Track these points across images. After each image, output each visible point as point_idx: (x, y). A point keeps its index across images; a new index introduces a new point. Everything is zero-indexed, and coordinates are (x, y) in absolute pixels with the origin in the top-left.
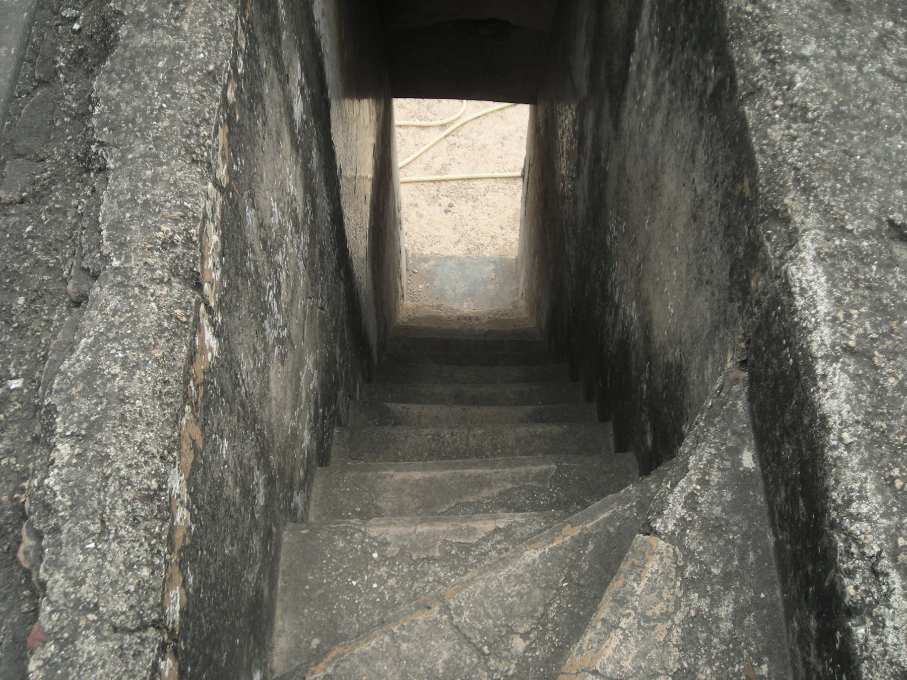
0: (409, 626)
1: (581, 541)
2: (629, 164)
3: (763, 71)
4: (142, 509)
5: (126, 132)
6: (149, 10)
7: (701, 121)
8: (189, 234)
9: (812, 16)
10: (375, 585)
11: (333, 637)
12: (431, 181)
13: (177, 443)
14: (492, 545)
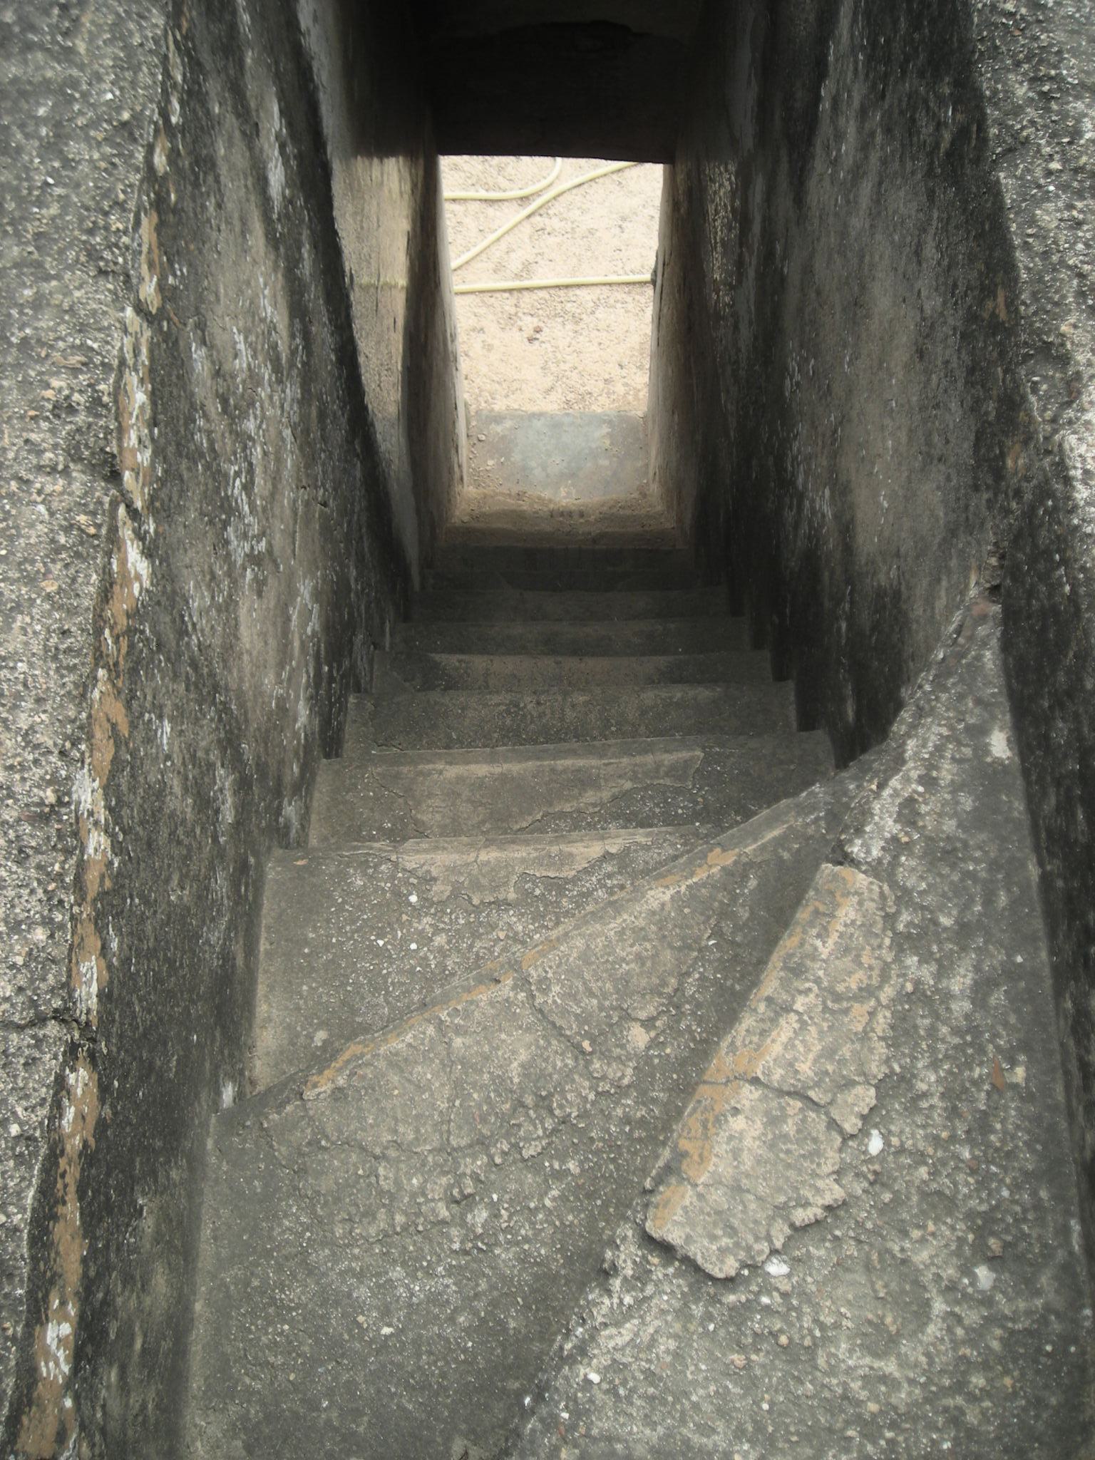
0: (465, 1010)
1: (736, 875)
2: (819, 264)
3: (1031, 112)
4: (32, 836)
7: (931, 195)
8: (97, 391)
10: (413, 946)
11: (349, 1028)
12: (504, 291)
13: (86, 730)
14: (599, 880)
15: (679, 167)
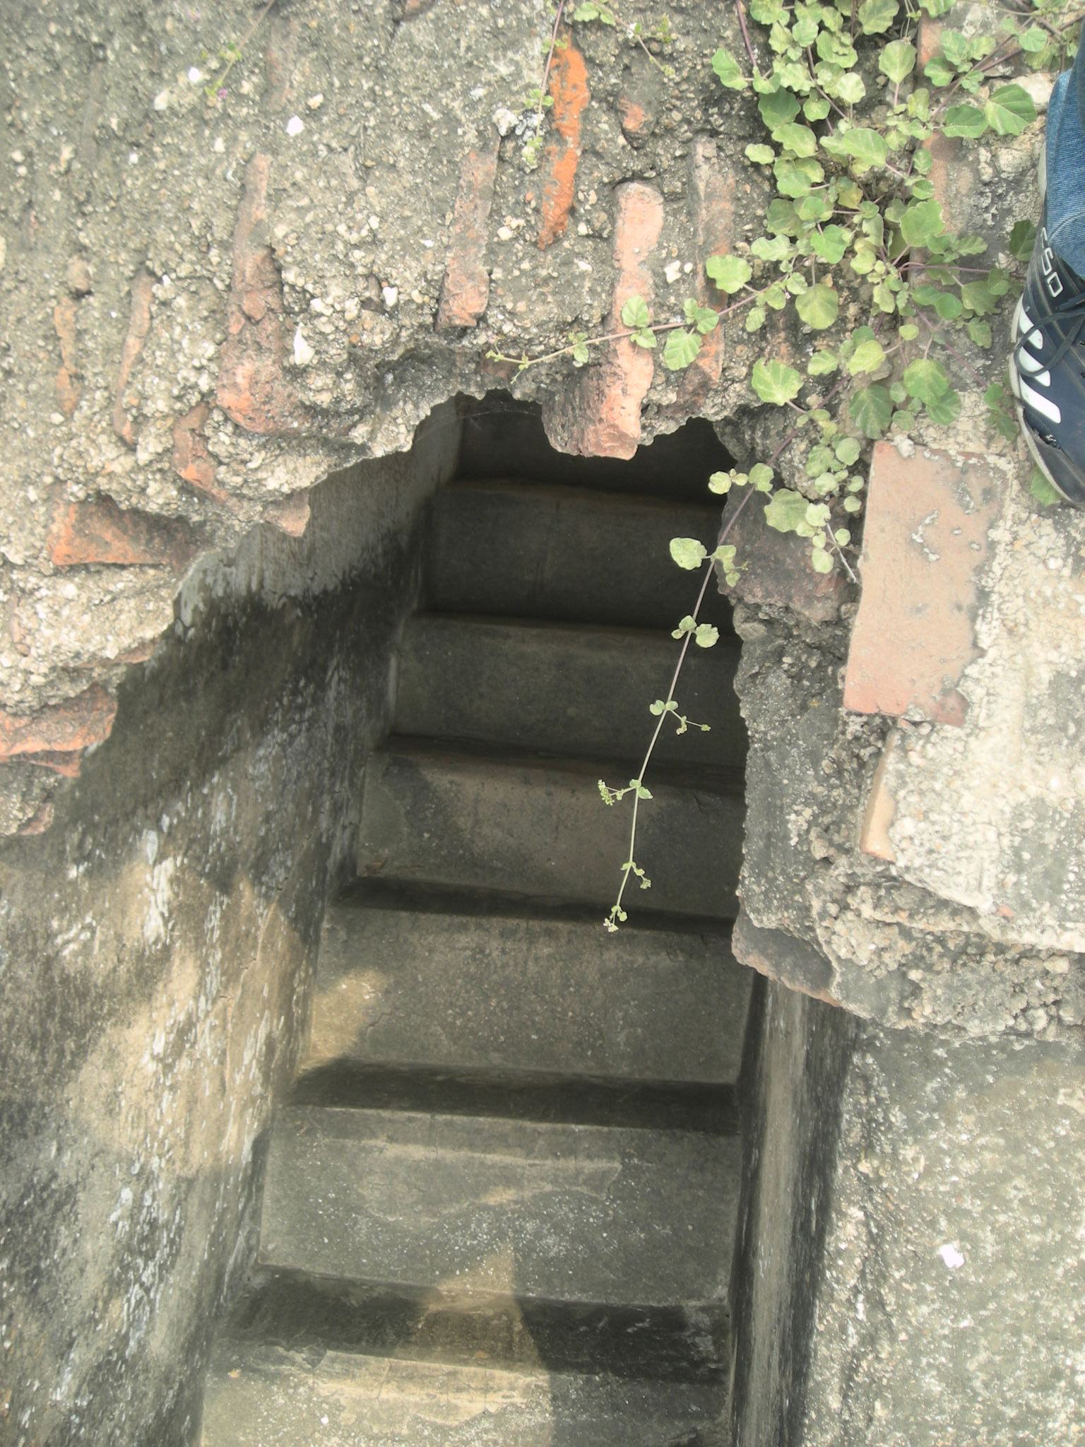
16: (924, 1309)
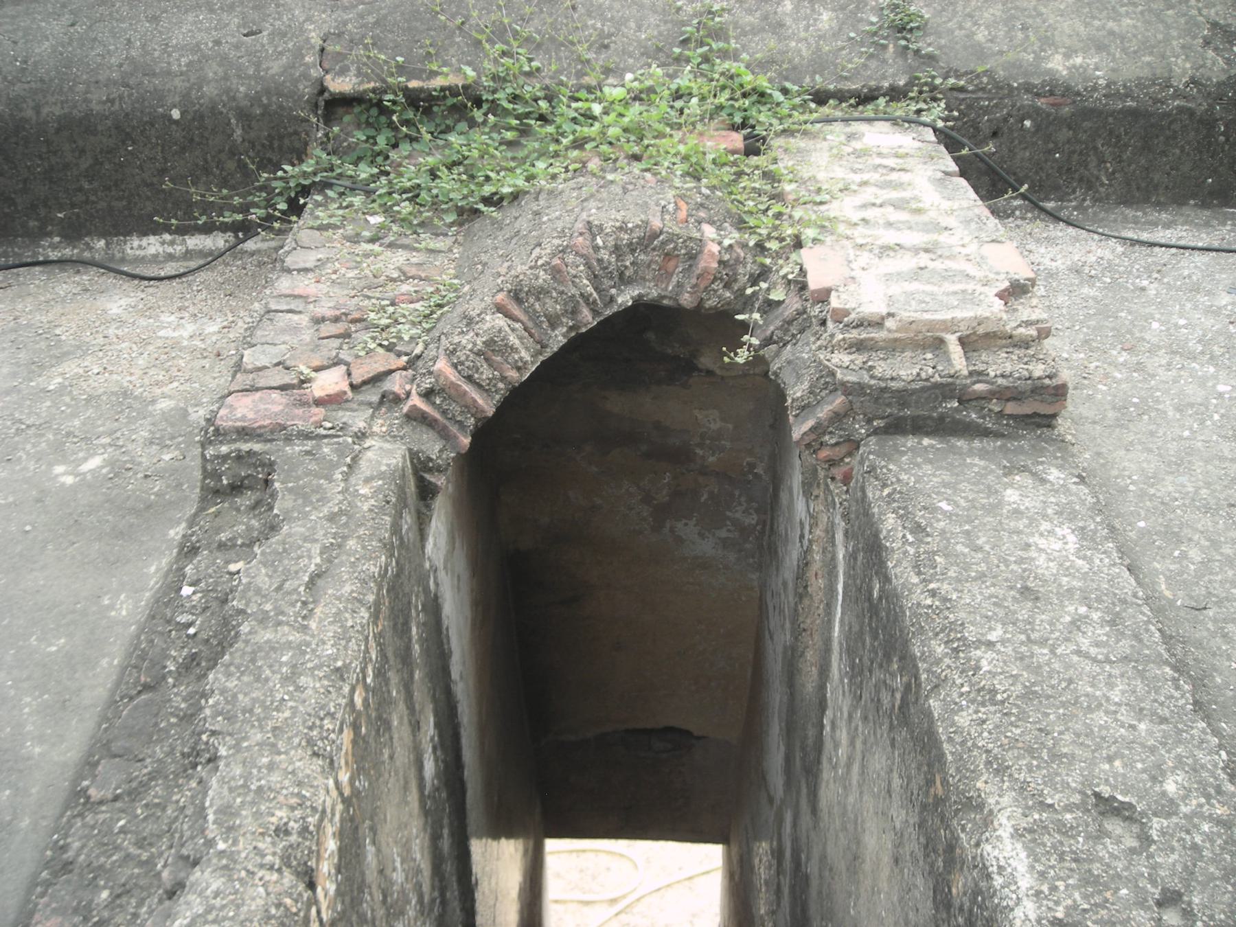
2: (830, 849)
3: (947, 661)
5: (243, 721)
6: (275, 608)
9: (995, 604)
15: (733, 846)
16: (942, 524)
